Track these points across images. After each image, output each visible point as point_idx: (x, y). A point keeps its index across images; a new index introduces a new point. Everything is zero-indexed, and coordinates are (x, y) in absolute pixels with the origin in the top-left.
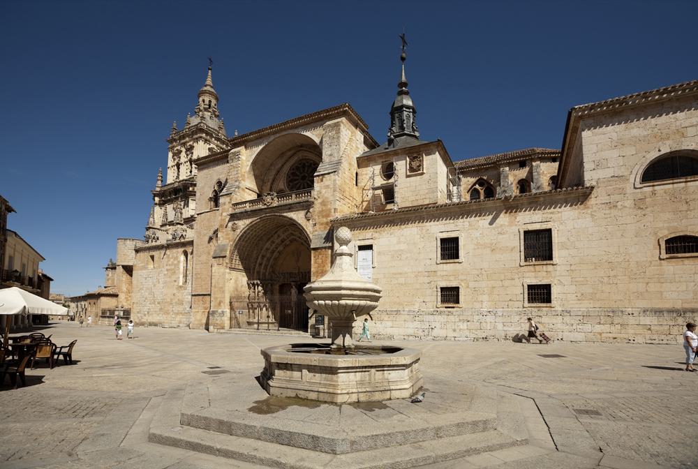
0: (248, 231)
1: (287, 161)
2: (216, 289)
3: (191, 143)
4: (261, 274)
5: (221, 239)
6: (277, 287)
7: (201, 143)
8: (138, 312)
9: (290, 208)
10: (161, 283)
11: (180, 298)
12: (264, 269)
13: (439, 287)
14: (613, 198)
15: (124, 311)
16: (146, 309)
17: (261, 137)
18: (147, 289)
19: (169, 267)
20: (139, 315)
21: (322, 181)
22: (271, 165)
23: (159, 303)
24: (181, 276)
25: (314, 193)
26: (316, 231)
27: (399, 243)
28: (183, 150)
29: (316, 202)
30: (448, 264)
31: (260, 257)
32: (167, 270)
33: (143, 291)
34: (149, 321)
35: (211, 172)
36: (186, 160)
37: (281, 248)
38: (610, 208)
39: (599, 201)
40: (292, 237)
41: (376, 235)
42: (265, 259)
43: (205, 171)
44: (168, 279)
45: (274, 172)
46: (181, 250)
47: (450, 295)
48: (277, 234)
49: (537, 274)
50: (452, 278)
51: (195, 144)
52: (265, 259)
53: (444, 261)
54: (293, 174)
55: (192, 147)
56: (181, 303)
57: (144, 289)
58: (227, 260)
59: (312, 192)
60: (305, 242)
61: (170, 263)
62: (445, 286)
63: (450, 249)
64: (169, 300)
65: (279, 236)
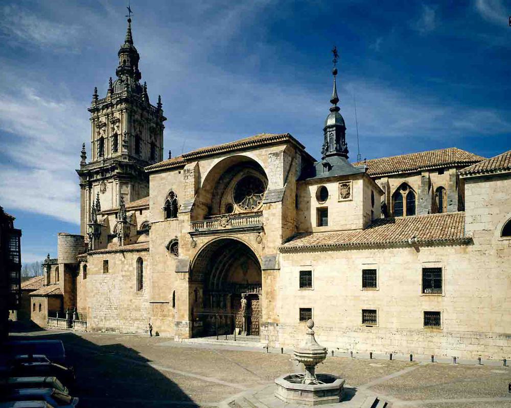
4: (215, 284)
5: (182, 255)
8: (95, 317)
10: (117, 288)
14: (485, 247)
19: (124, 273)
20: (96, 320)
21: (269, 209)
22: (220, 180)
23: (116, 309)
32: (123, 276)
34: (106, 326)
38: (481, 255)
39: (474, 249)
41: (314, 263)
46: (136, 256)
47: (369, 316)
49: (431, 303)
56: (138, 309)
58: (187, 275)
63: (369, 278)
64: (125, 306)
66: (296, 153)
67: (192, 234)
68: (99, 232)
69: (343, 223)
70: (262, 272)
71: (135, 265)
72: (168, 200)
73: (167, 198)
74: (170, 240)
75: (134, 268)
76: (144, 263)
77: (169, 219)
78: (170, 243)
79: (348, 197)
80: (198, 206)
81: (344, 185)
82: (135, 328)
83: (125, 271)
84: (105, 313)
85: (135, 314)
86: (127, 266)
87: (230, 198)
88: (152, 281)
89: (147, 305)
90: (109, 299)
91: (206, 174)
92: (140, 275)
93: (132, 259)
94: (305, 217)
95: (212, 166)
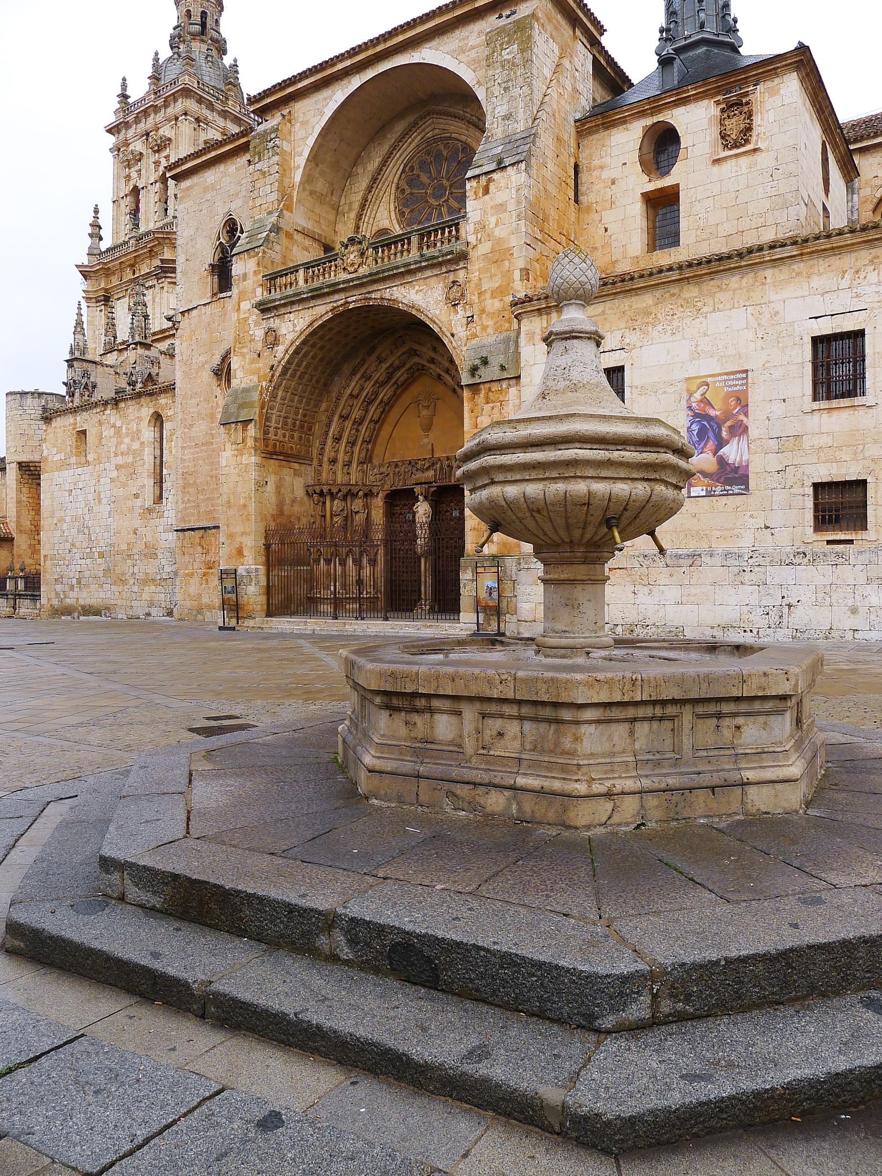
0: (305, 349)
1: (394, 148)
2: (231, 513)
6: (378, 502)
9: (408, 272)
10: (104, 501)
11: (149, 539)
12: (346, 453)
13: (809, 483)
15: (26, 578)
16: (72, 572)
18: (76, 519)
19: (120, 460)
20: (59, 588)
21: (486, 191)
23: (102, 555)
24: (149, 482)
25: (468, 230)
26: (474, 336)
27: (696, 355)
29: (473, 254)
30: (835, 414)
31: (336, 418)
32: (118, 467)
33: (65, 527)
34: (81, 602)
37: (385, 393)
40: (416, 360)
41: (632, 338)
42: (348, 424)
44: (121, 492)
45: (363, 183)
46: (146, 410)
48: (377, 353)
50: (845, 455)
52: (348, 424)
53: (824, 404)
54: (413, 181)
56: (150, 552)
57: (68, 519)
58: (252, 430)
59: (462, 226)
60: (447, 371)
61: (123, 447)
62: (825, 480)
64: (124, 547)
65: (381, 360)
66: (575, 37)
67: (265, 308)
68: (92, 379)
69: (729, 228)
70: (466, 394)
71: (148, 434)
75: (142, 443)
76: (167, 426)
77: (222, 295)
79: (747, 141)
80: (289, 236)
81: (730, 106)
82: (144, 604)
83: (122, 453)
84: (78, 568)
85: (142, 568)
86: (127, 440)
87: (386, 213)
88: (181, 471)
89: (172, 536)
90: (86, 531)
91: (311, 141)
92: (158, 461)
93: (140, 419)
94: (606, 230)
95: (329, 112)
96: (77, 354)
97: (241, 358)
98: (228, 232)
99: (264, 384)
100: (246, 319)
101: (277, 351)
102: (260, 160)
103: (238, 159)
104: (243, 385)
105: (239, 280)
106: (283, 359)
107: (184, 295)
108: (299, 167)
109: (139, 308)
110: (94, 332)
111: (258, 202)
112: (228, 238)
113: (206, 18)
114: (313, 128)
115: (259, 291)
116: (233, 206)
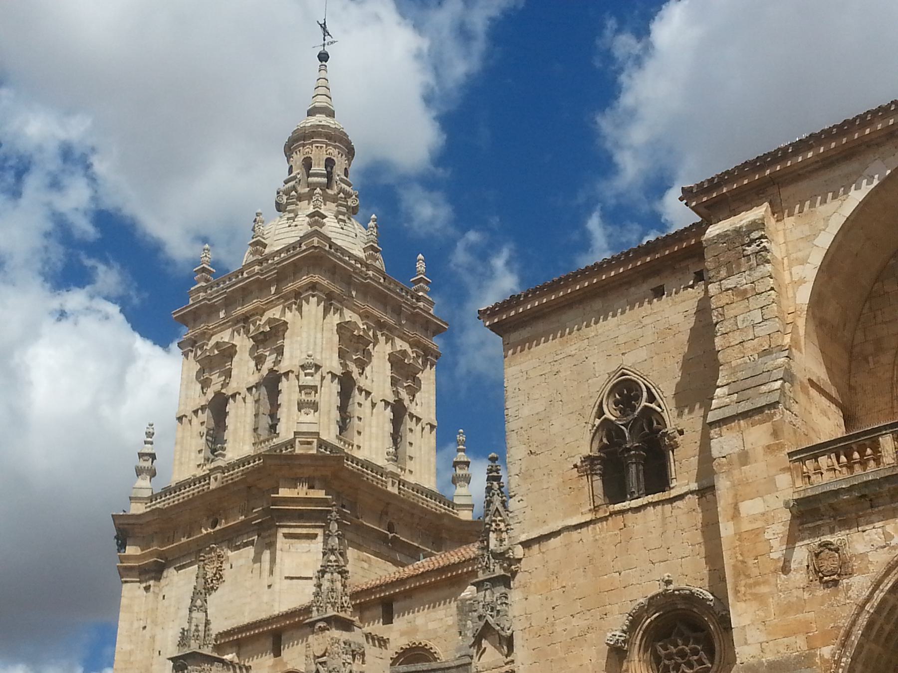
3: (275, 313)
5: (755, 635)
7: (313, 308)
17: (849, 154)
22: (879, 278)
28: (243, 343)
35: (572, 349)
36: (254, 379)
43: (545, 350)
51: (289, 316)
55: (278, 329)
72: (606, 419)
73: (600, 413)
74: (631, 607)
77: (618, 507)
78: (635, 621)
96: (194, 646)
97: (755, 605)
98: (616, 403)
99: (826, 652)
100: (758, 533)
101: (849, 587)
102: (730, 274)
103: (633, 289)
104: (770, 657)
105: (730, 463)
106: (868, 599)
107: (528, 510)
108: (802, 281)
109: (332, 558)
110: (132, 624)
111: (735, 338)
112: (618, 413)
113: (332, 168)
114: (827, 220)
115: (783, 480)
116: (628, 361)
